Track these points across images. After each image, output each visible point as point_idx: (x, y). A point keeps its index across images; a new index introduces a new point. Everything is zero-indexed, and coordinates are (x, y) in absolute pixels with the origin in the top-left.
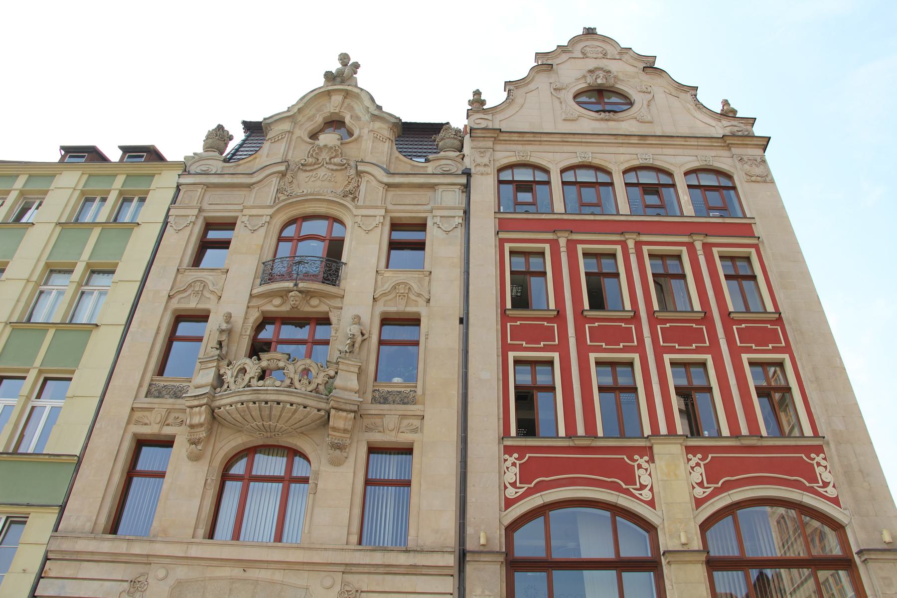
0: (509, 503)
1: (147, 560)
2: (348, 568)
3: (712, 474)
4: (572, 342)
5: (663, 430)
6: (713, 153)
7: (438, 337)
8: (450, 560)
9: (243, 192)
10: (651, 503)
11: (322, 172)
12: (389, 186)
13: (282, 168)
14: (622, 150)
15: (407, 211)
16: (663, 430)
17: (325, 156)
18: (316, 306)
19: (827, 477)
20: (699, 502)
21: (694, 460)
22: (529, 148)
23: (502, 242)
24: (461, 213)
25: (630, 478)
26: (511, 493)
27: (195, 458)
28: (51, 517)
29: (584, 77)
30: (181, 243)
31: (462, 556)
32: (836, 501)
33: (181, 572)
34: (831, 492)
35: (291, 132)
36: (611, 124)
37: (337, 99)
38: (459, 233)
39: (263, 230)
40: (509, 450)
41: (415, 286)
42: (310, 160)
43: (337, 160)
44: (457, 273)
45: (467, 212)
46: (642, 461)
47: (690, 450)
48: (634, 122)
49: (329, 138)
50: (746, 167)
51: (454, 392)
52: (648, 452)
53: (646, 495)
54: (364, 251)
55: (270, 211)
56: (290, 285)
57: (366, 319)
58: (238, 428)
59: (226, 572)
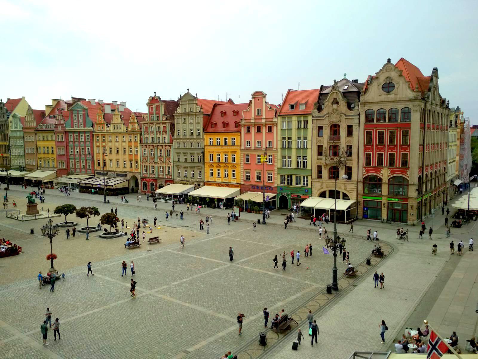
0: (364, 175)
1: (322, 182)
2: (345, 183)
3: (391, 172)
4: (374, 150)
5: (386, 166)
6: (408, 103)
7: (355, 150)
8: (356, 183)
9: (323, 120)
10: (382, 176)
11: (335, 115)
12: (346, 119)
13: (328, 115)
14: (389, 104)
15: (349, 124)
16: (386, 166)
17: (335, 111)
18: (337, 144)
19: (408, 173)
20: (389, 176)
21: (389, 170)
22: (371, 105)
23: (365, 130)
24: (358, 125)
25: (380, 172)
26: (364, 174)
27: (326, 169)
28: (311, 176)
29: (385, 80)
30: (315, 132)
31: (358, 182)
32: (408, 177)
33: (327, 183)
34: (408, 176)
35: (328, 104)
36: (389, 96)
37: (335, 94)
38: (358, 129)
39: (327, 130)
40: (364, 168)
41: (351, 140)
42: (332, 112)
43: (337, 112)
44: (357, 138)
45: (359, 124)
46: (382, 170)
47: (389, 168)
48: (393, 95)
49: (335, 106)
50: (414, 108)
51: (357, 160)
52: (383, 168)
53: (382, 175)
54: (343, 132)
55: (328, 125)
56: (333, 142)
57: (344, 147)
58: (329, 165)
59: (331, 183)
